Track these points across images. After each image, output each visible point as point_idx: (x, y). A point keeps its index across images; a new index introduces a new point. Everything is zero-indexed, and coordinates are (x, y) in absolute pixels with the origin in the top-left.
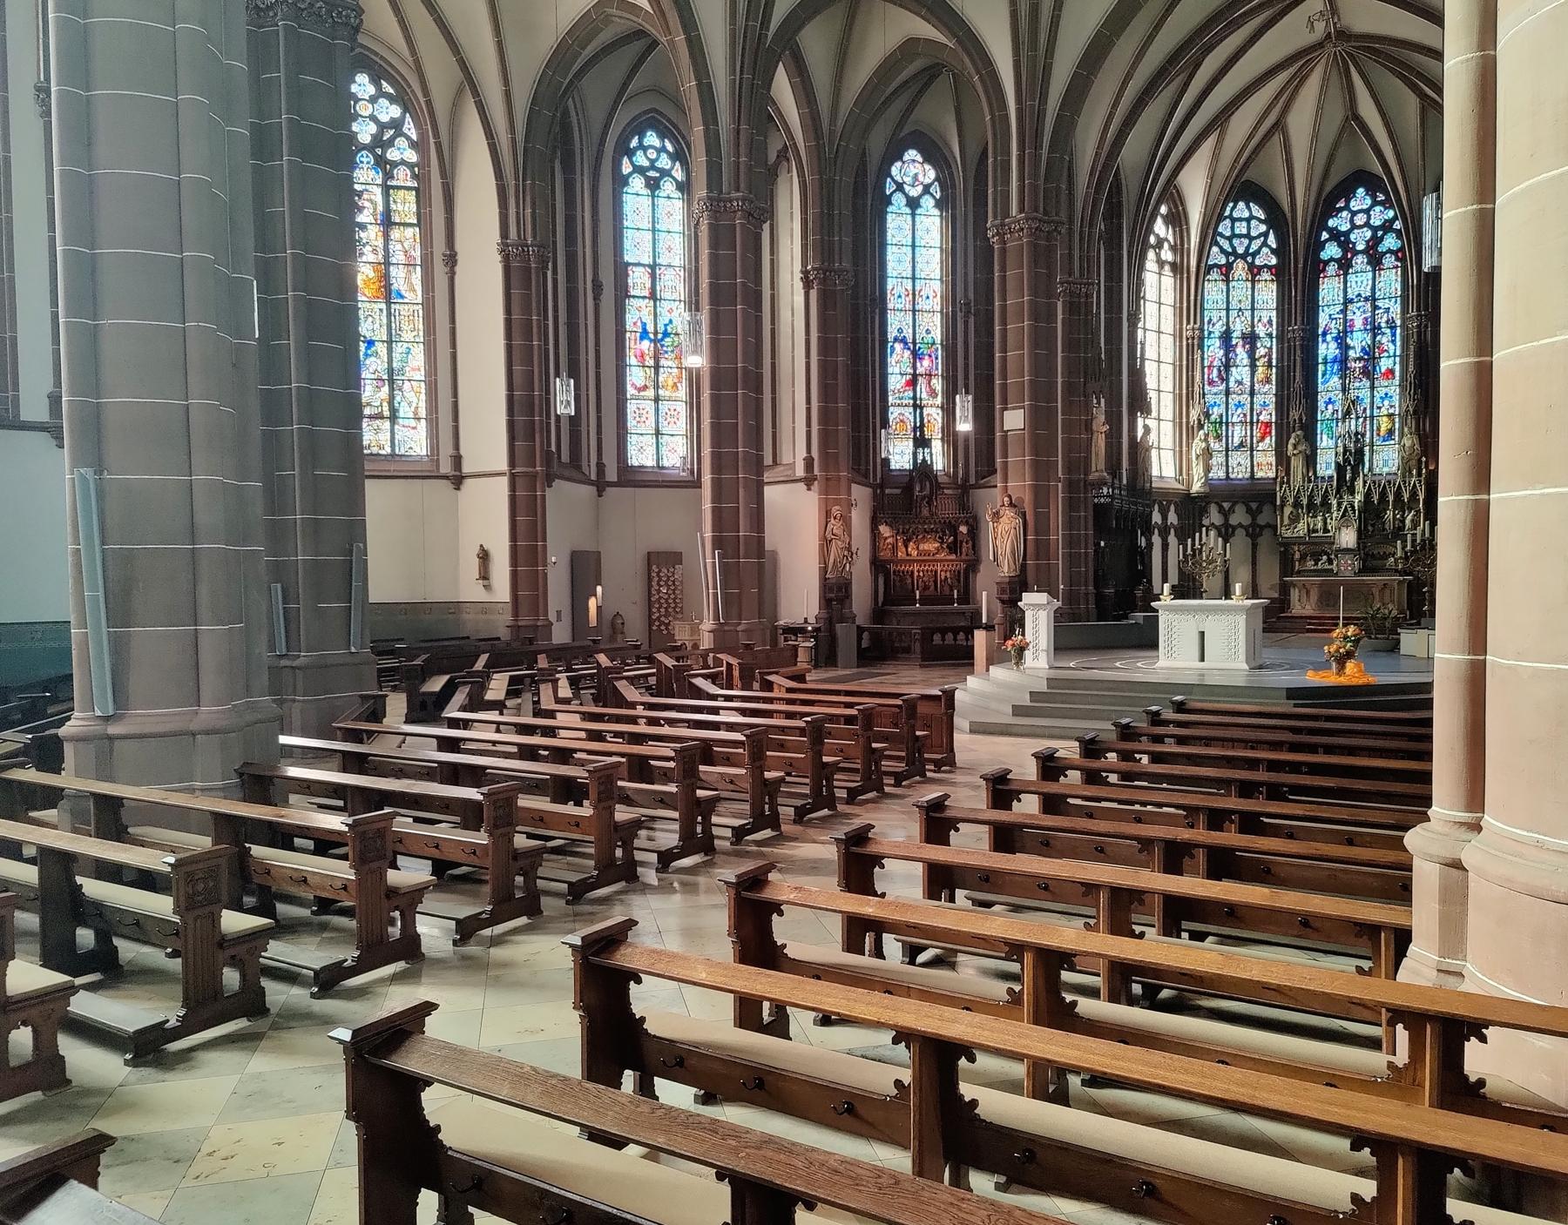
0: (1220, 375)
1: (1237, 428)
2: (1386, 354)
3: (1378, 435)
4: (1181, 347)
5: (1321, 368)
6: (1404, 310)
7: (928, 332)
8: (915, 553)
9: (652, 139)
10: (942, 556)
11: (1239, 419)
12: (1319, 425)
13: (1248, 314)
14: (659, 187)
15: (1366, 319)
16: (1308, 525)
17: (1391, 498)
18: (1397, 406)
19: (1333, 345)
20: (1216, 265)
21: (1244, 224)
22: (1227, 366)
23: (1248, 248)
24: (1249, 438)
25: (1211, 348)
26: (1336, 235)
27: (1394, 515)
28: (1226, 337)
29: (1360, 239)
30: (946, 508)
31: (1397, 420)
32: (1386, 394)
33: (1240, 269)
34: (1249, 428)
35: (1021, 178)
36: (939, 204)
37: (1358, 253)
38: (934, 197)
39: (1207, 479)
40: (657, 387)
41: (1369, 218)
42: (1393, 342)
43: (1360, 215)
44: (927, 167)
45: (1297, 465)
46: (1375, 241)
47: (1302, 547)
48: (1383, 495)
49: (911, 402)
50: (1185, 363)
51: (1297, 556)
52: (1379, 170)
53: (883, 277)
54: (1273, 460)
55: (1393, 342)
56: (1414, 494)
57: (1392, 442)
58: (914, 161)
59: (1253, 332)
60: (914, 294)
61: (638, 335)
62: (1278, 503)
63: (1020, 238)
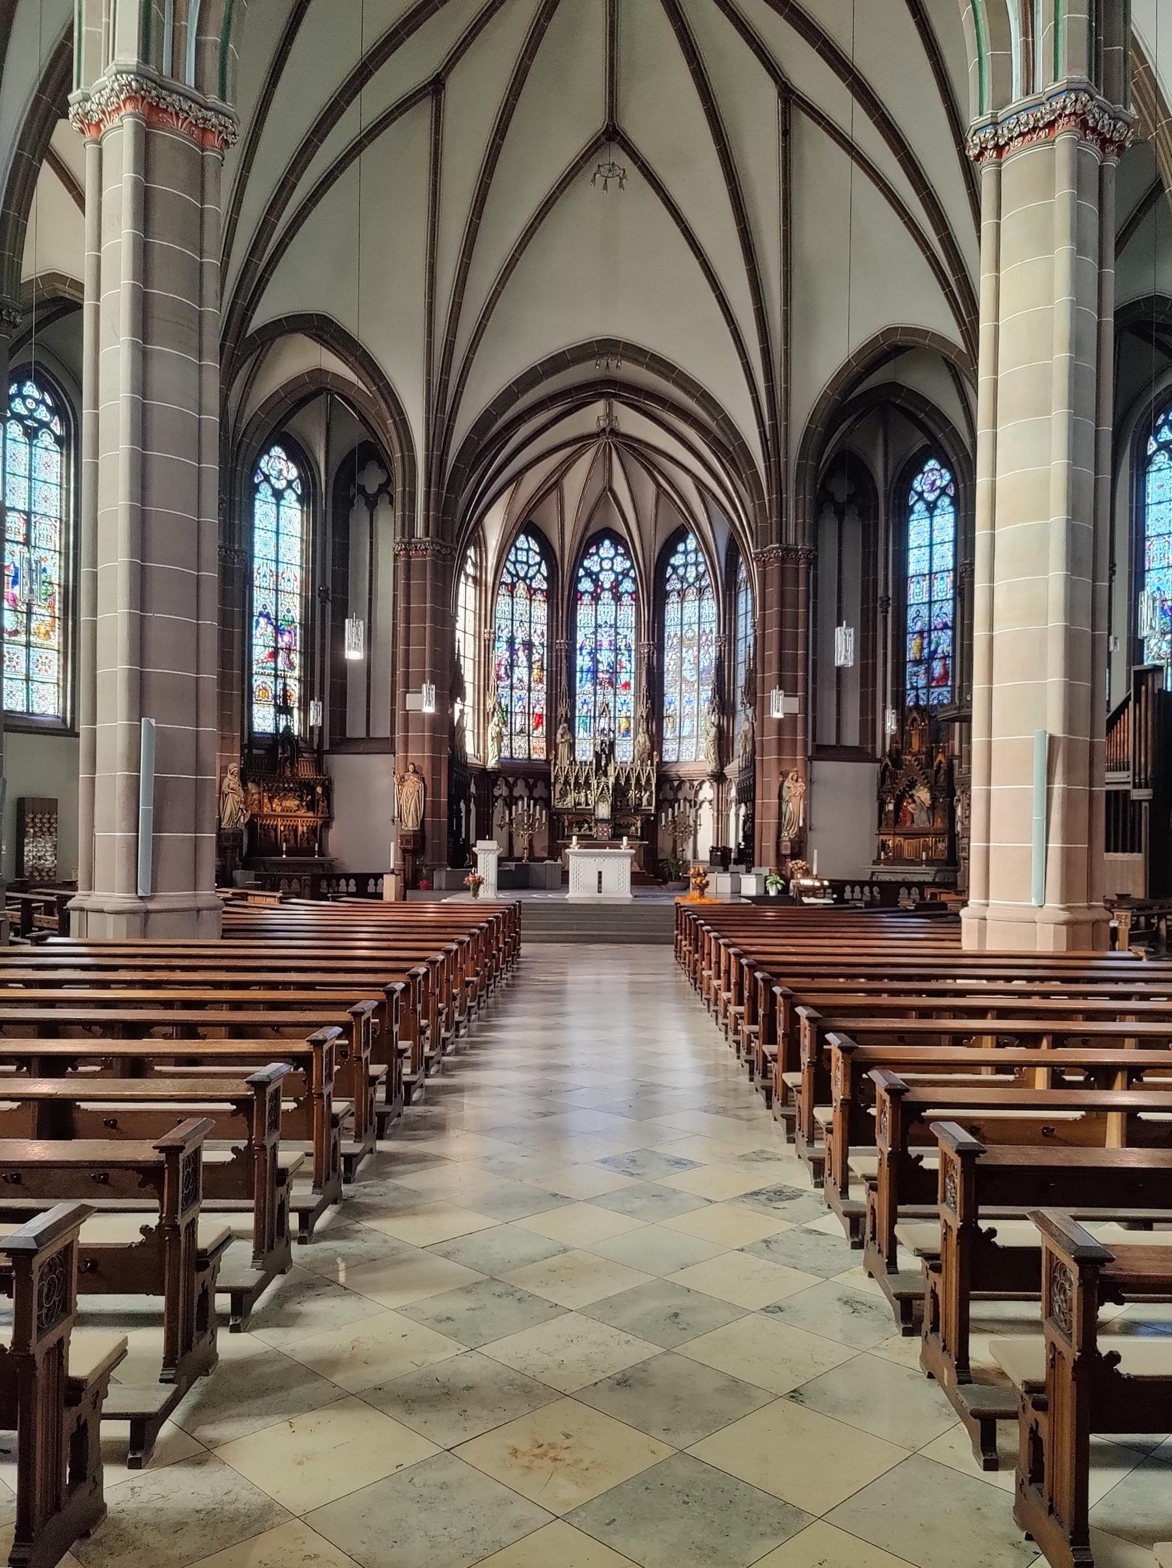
0: (506, 673)
1: (519, 717)
2: (624, 670)
4: (479, 646)
5: (578, 675)
6: (638, 638)
7: (289, 611)
8: (279, 809)
9: (30, 389)
10: (302, 812)
13: (527, 625)
14: (36, 437)
15: (610, 641)
17: (633, 782)
18: (632, 709)
19: (587, 658)
20: (504, 583)
21: (525, 553)
22: (512, 665)
23: (527, 572)
25: (500, 650)
26: (589, 574)
28: (511, 642)
29: (607, 579)
30: (306, 771)
31: (632, 721)
33: (521, 588)
35: (427, 509)
36: (301, 499)
37: (603, 590)
38: (296, 492)
39: (499, 758)
40: (28, 632)
41: (613, 564)
42: (630, 661)
43: (607, 561)
44: (291, 465)
45: (563, 750)
46: (616, 584)
47: (570, 817)
48: (628, 779)
49: (273, 672)
50: (482, 659)
51: (566, 823)
52: (623, 531)
53: (252, 557)
54: (544, 745)
55: (630, 661)
56: (648, 779)
58: (279, 457)
59: (530, 640)
60: (277, 576)
61: (11, 579)
62: (552, 780)
63: (425, 556)
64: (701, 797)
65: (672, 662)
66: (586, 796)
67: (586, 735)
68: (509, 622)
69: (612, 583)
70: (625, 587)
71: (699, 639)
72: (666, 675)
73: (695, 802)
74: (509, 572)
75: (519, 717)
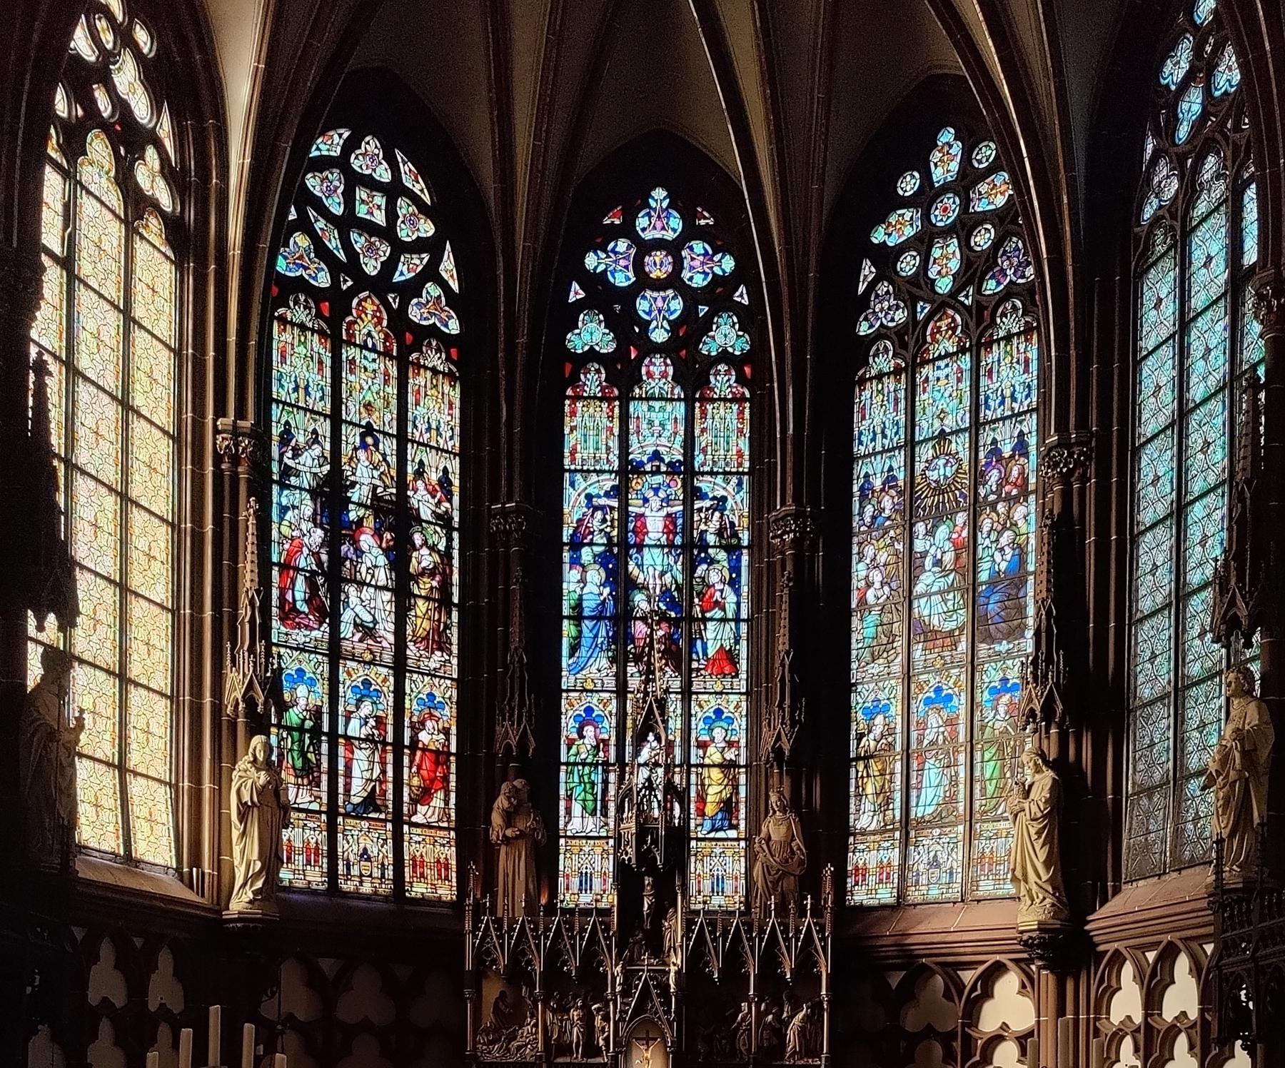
1: (361, 759)
3: (701, 813)
5: (568, 628)
11: (365, 732)
12: (562, 775)
17: (752, 970)
24: (390, 786)
27: (761, 1016)
31: (742, 779)
32: (719, 712)
34: (390, 757)
48: (734, 959)
56: (806, 961)
57: (732, 834)
62: (469, 965)
64: (989, 1021)
65: (877, 577)
66: (588, 1020)
67: (591, 825)
68: (325, 427)
69: (675, 325)
70: (720, 340)
71: (978, 477)
72: (855, 622)
73: (968, 1041)
74: (321, 251)
75: (361, 759)
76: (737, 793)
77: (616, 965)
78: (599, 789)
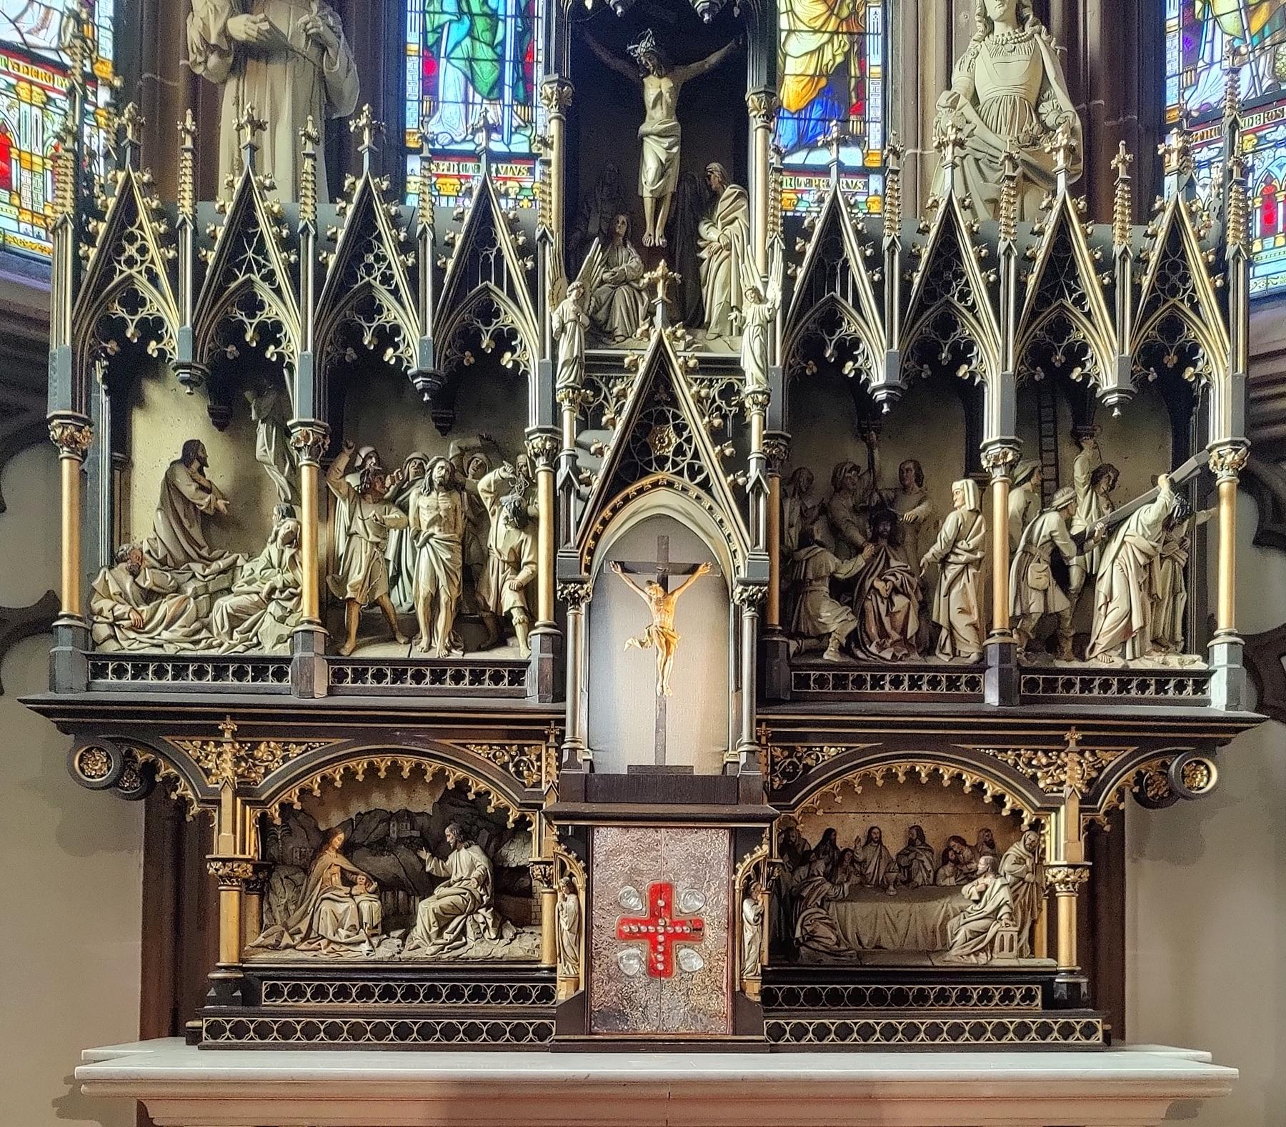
16: (330, 568)
76: (862, 54)
77: (558, 299)
78: (507, 31)
